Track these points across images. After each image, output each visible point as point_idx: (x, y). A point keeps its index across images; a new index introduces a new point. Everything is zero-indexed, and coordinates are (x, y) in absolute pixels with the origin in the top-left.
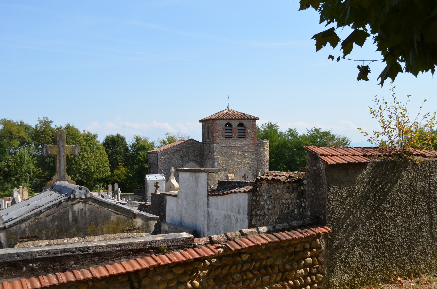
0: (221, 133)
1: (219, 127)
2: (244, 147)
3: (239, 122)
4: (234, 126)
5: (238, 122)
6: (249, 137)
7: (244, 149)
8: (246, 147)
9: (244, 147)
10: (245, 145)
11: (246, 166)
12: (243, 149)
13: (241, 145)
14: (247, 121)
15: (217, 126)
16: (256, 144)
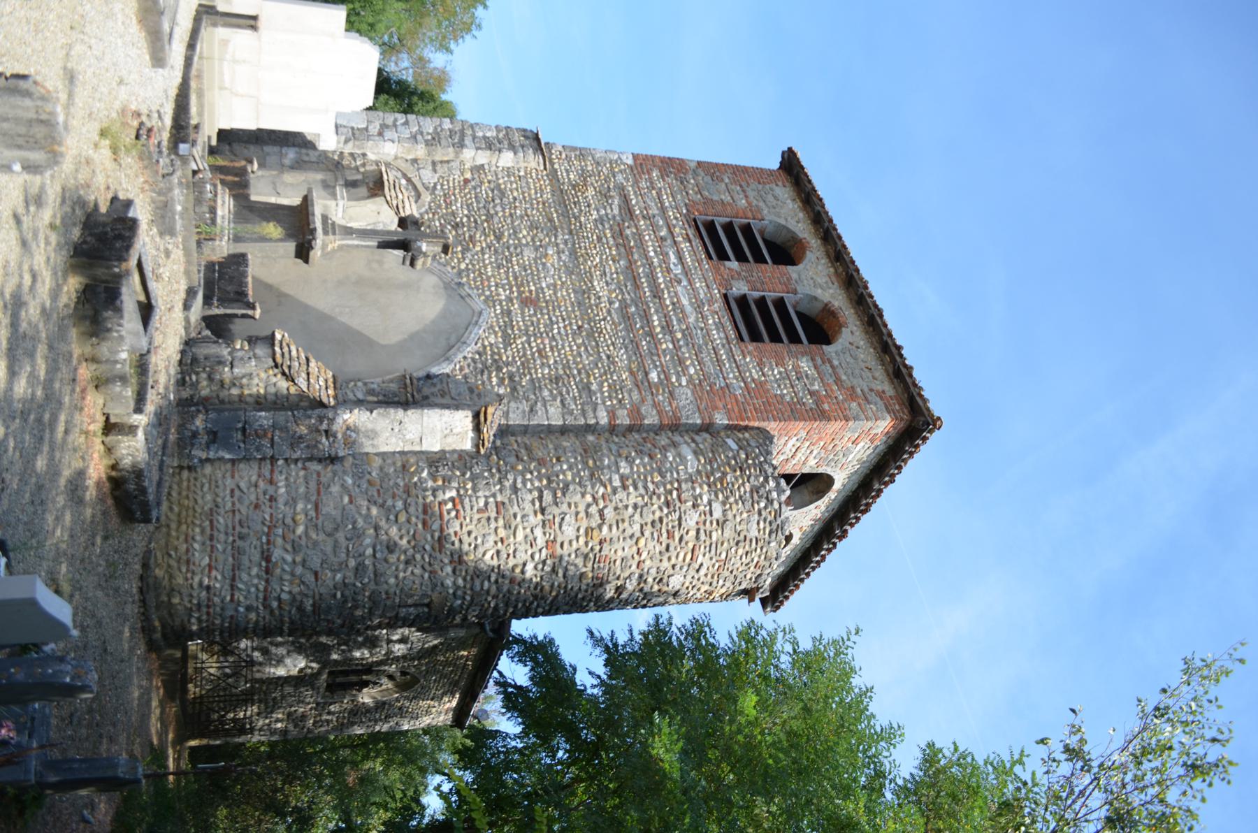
0: (715, 198)
1: (751, 194)
2: (668, 328)
3: (836, 304)
4: (794, 276)
5: (832, 296)
6: (761, 365)
7: (652, 328)
8: (674, 341)
9: (668, 328)
10: (683, 332)
11: (506, 336)
12: (646, 317)
13: (676, 305)
14: (866, 354)
15: (754, 185)
16: (721, 419)
